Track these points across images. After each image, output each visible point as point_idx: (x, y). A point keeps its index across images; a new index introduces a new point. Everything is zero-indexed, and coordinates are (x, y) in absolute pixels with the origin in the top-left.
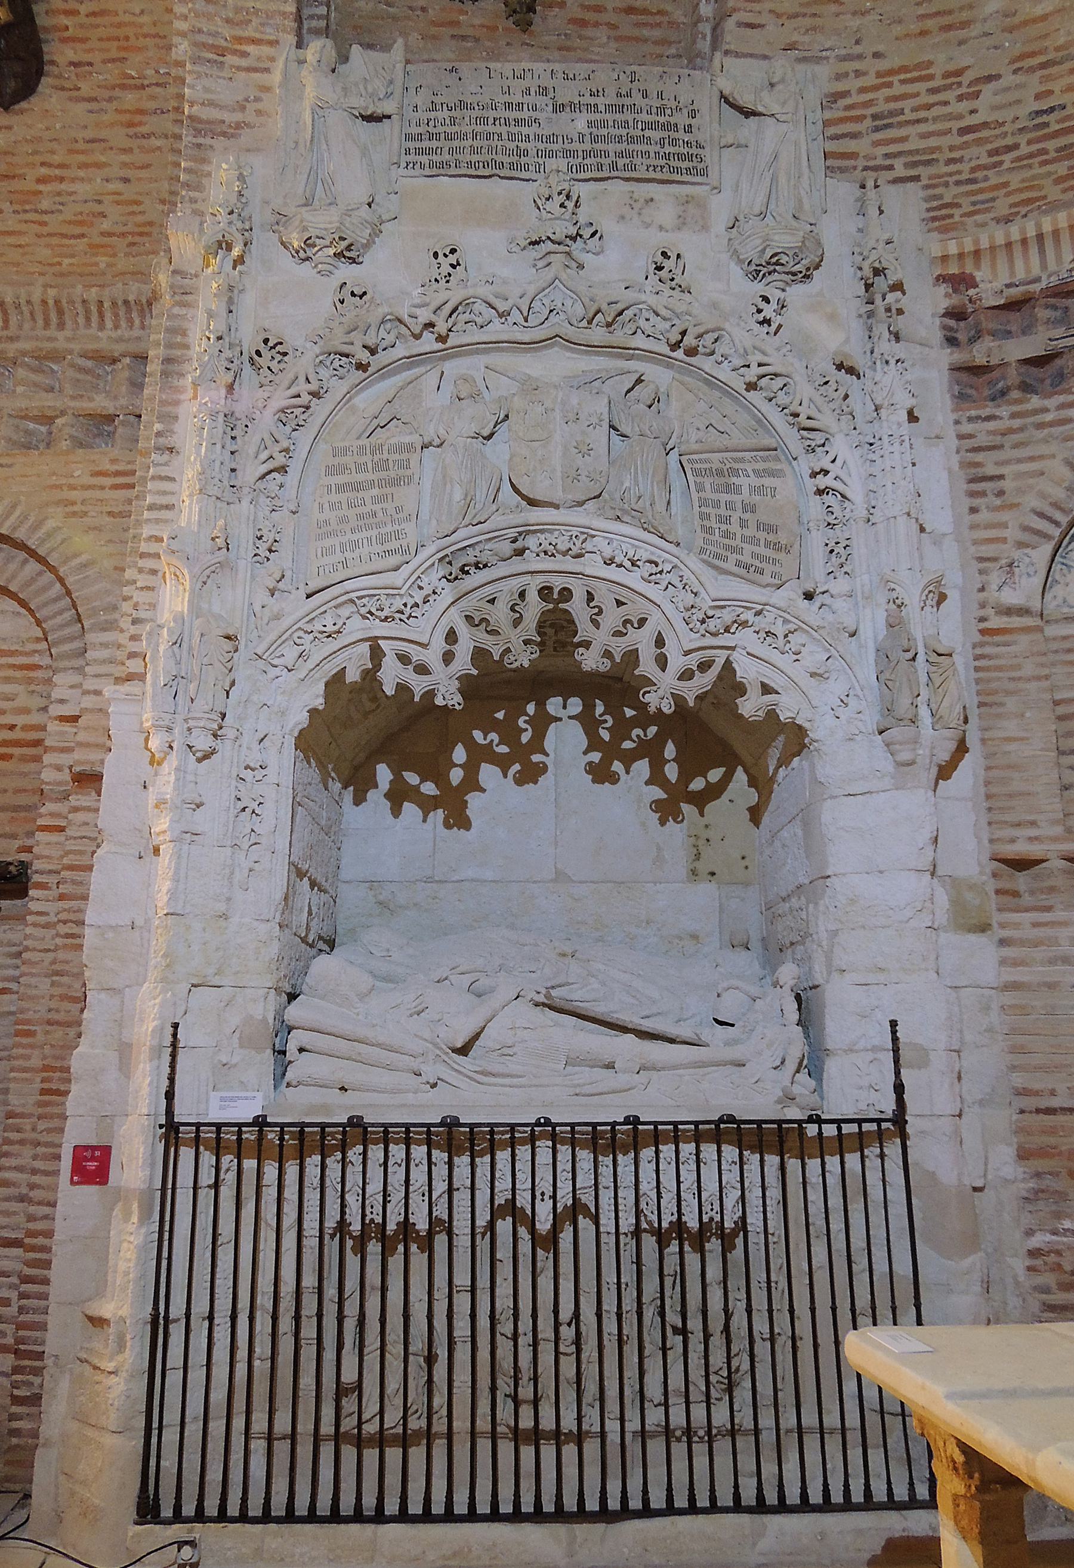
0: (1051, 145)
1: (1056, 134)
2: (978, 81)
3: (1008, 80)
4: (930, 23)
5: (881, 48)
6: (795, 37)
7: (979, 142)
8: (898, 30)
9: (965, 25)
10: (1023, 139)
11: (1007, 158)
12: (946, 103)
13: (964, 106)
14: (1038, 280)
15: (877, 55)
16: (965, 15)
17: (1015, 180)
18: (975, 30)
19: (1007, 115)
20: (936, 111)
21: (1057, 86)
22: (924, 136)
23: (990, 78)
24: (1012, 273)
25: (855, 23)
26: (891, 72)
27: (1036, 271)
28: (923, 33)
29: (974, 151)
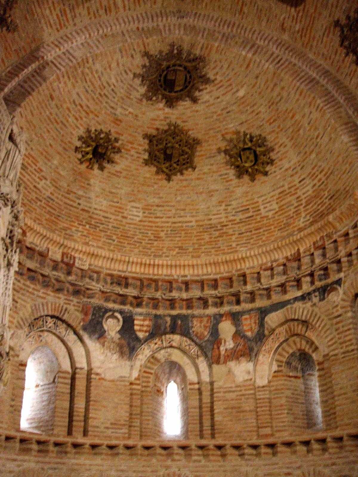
0: (48, 208)
1: (50, 206)
2: (43, 177)
3: (48, 182)
4: (44, 153)
5: (34, 148)
6: (24, 127)
7: (36, 193)
8: (38, 147)
9: (49, 160)
10: (44, 201)
11: (39, 203)
12: (35, 176)
13: (38, 180)
14: (37, 246)
15: (32, 149)
16: (50, 158)
17: (38, 210)
18: (50, 164)
19: (44, 191)
20: (33, 176)
21: (55, 194)
22: (28, 180)
23: (46, 179)
24: (34, 239)
25: (34, 136)
26: (31, 156)
27: (38, 243)
28: (42, 153)
29: (34, 194)
